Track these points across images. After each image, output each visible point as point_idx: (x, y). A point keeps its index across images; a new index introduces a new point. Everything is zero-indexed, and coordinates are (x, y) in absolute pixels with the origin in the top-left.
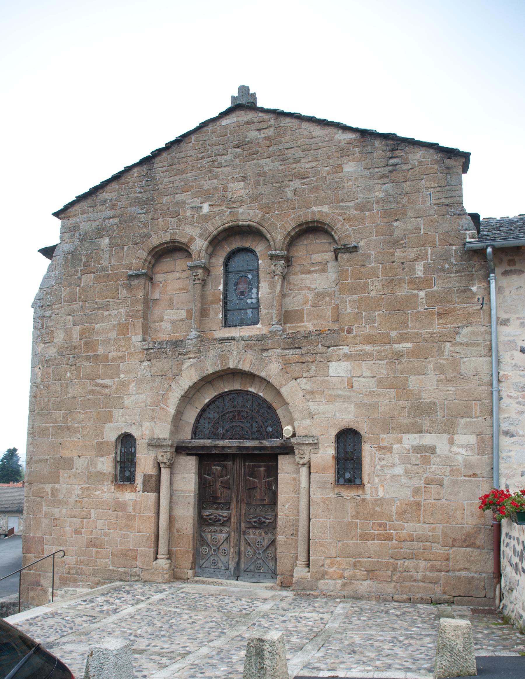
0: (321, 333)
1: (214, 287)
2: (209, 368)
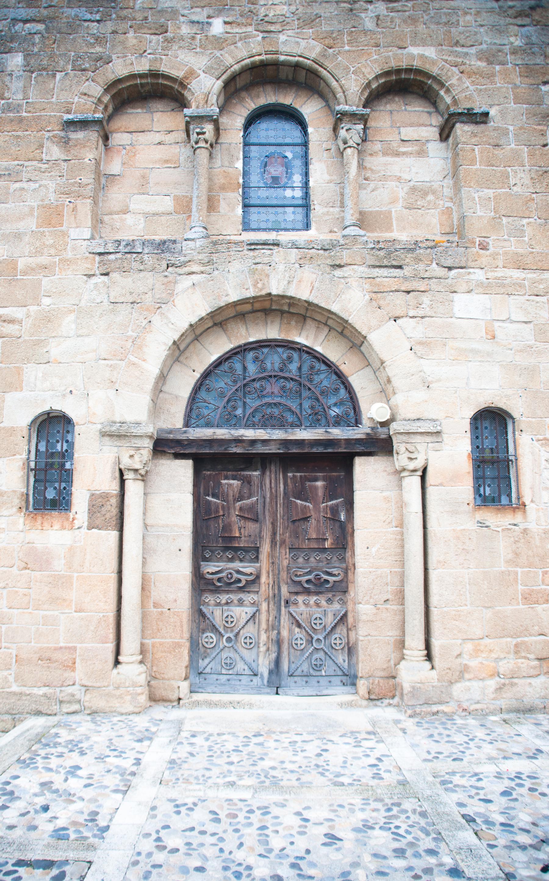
0: (437, 244)
1: (226, 164)
2: (230, 292)
